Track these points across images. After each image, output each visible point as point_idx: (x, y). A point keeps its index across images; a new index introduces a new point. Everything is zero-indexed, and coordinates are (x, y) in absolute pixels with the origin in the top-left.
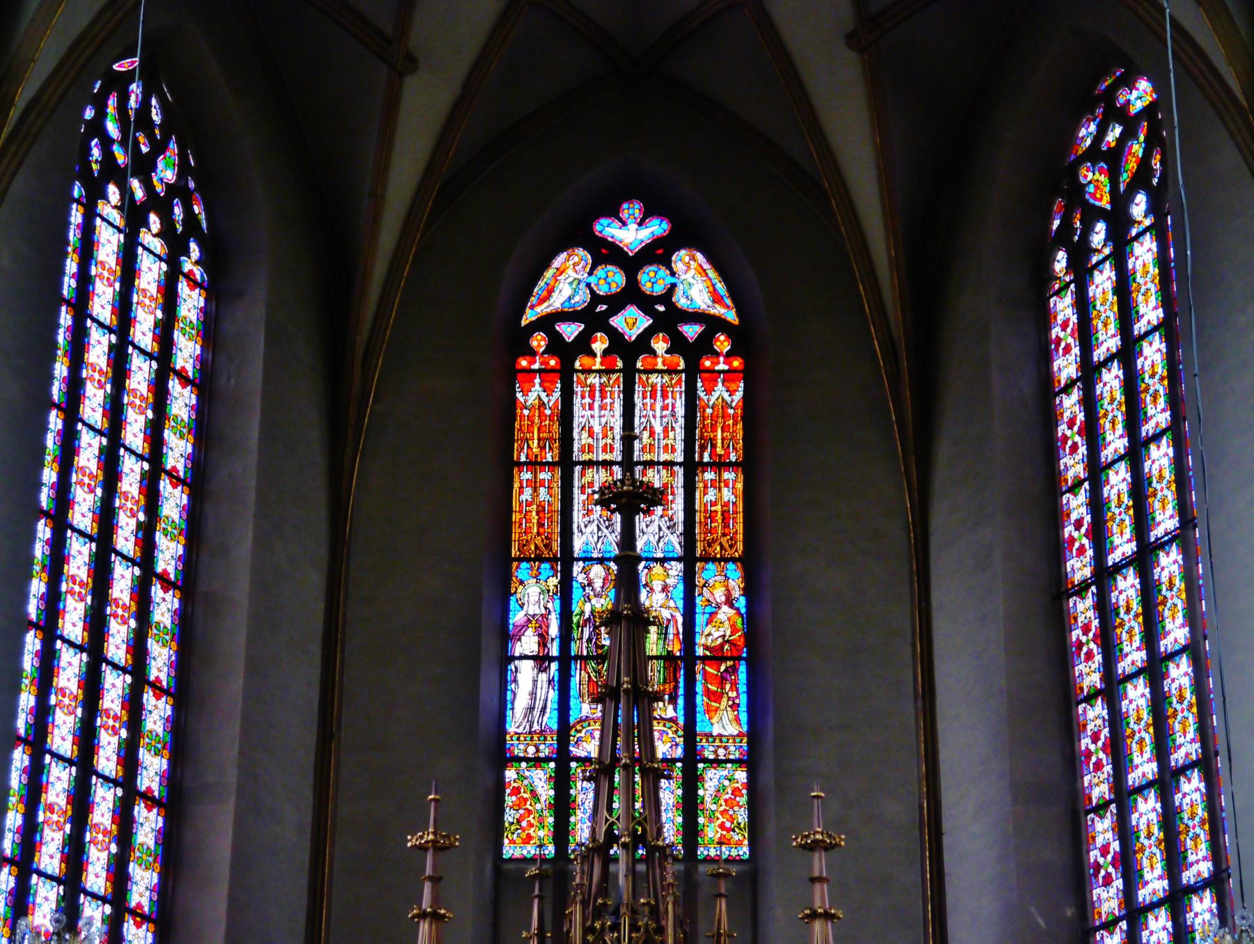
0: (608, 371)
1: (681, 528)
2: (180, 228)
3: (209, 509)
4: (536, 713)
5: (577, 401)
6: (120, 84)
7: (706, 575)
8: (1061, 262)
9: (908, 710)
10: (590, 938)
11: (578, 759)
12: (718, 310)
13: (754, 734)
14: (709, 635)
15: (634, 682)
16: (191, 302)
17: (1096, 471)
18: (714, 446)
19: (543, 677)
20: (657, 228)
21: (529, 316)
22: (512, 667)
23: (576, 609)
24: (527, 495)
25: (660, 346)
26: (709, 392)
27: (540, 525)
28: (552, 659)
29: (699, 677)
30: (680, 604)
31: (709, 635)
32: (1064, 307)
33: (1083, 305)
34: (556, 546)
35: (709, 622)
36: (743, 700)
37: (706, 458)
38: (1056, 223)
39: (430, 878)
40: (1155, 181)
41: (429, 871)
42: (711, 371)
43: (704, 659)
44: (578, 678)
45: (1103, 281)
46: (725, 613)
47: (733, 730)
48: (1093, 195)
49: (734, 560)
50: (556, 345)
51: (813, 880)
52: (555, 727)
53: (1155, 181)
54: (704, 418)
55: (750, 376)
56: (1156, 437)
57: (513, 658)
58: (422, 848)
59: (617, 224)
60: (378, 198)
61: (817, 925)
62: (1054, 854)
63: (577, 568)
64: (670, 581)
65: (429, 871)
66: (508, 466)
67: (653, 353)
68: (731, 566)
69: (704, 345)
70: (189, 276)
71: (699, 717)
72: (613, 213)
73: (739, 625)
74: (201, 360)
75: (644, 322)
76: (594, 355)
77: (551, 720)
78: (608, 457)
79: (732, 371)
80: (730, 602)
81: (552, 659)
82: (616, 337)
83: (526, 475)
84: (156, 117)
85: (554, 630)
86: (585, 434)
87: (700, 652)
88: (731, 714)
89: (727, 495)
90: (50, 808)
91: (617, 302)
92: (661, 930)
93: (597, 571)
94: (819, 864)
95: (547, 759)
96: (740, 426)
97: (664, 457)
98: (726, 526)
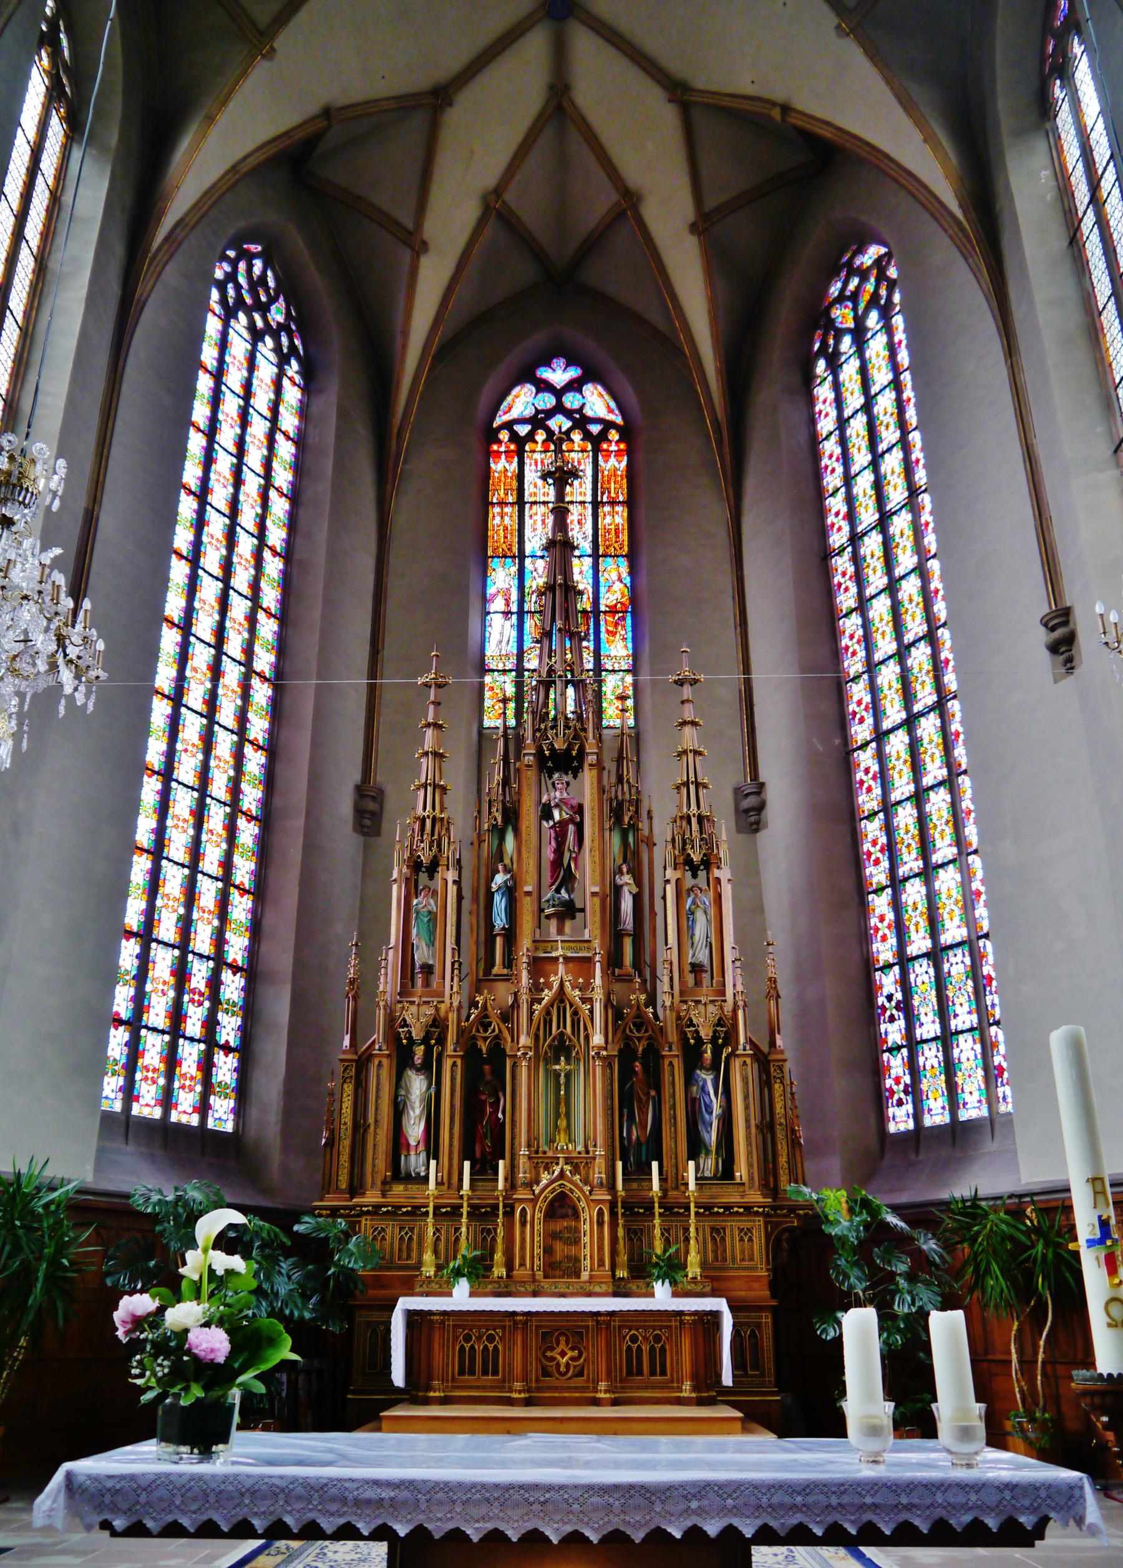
0: (546, 451)
1: (590, 538)
2: (285, 350)
3: (301, 511)
4: (504, 644)
5: (527, 468)
6: (250, 257)
7: (605, 565)
8: (821, 365)
9: (731, 636)
10: (538, 734)
11: (528, 670)
12: (611, 417)
13: (636, 656)
14: (607, 600)
15: (565, 579)
16: (292, 395)
17: (848, 480)
18: (609, 492)
19: (508, 623)
20: (573, 373)
21: (497, 422)
22: (488, 618)
23: (527, 584)
24: (498, 520)
25: (576, 436)
26: (606, 462)
27: (505, 537)
28: (512, 613)
29: (602, 623)
30: (591, 581)
31: (607, 600)
32: (824, 392)
33: (837, 386)
34: (515, 549)
35: (608, 591)
36: (630, 635)
37: (605, 499)
38: (817, 346)
39: (433, 703)
40: (883, 302)
41: (432, 698)
42: (607, 451)
43: (605, 612)
44: (529, 624)
45: (850, 371)
46: (618, 586)
47: (624, 653)
48: (841, 323)
49: (623, 556)
50: (514, 437)
51: (683, 702)
52: (515, 652)
53: (883, 302)
54: (603, 477)
55: (630, 452)
56: (889, 450)
57: (489, 613)
58: (427, 685)
59: (550, 370)
60: (406, 333)
61: (688, 729)
62: (827, 707)
63: (528, 561)
64: (585, 569)
65: (432, 698)
66: (486, 504)
67: (572, 441)
68: (621, 559)
69: (603, 436)
70: (291, 379)
71: (602, 645)
72: (548, 364)
73: (626, 592)
74: (298, 428)
75: (567, 424)
76: (536, 442)
77: (513, 648)
78: (546, 499)
79: (619, 450)
80: (620, 580)
81: (512, 613)
82: (550, 433)
83: (497, 510)
84: (271, 283)
85: (514, 596)
86: (532, 486)
87: (603, 608)
88: (621, 644)
89: (618, 520)
90: (195, 670)
91: (550, 413)
92: (585, 730)
93: (542, 509)
94: (687, 692)
95: (510, 671)
96: (625, 481)
97: (580, 499)
98: (617, 536)
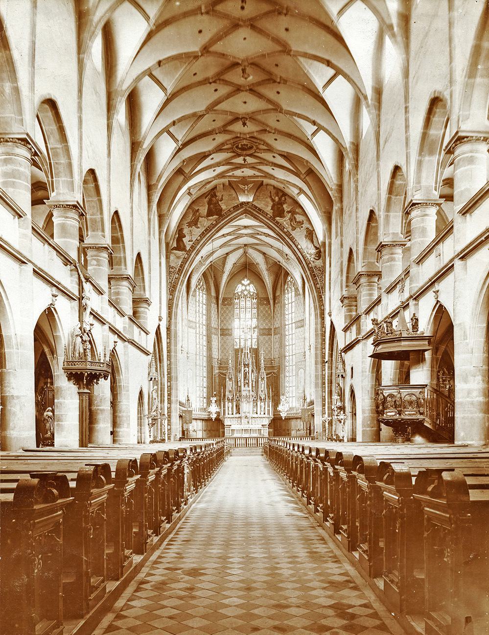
20: (248, 282)
82: (244, 294)
